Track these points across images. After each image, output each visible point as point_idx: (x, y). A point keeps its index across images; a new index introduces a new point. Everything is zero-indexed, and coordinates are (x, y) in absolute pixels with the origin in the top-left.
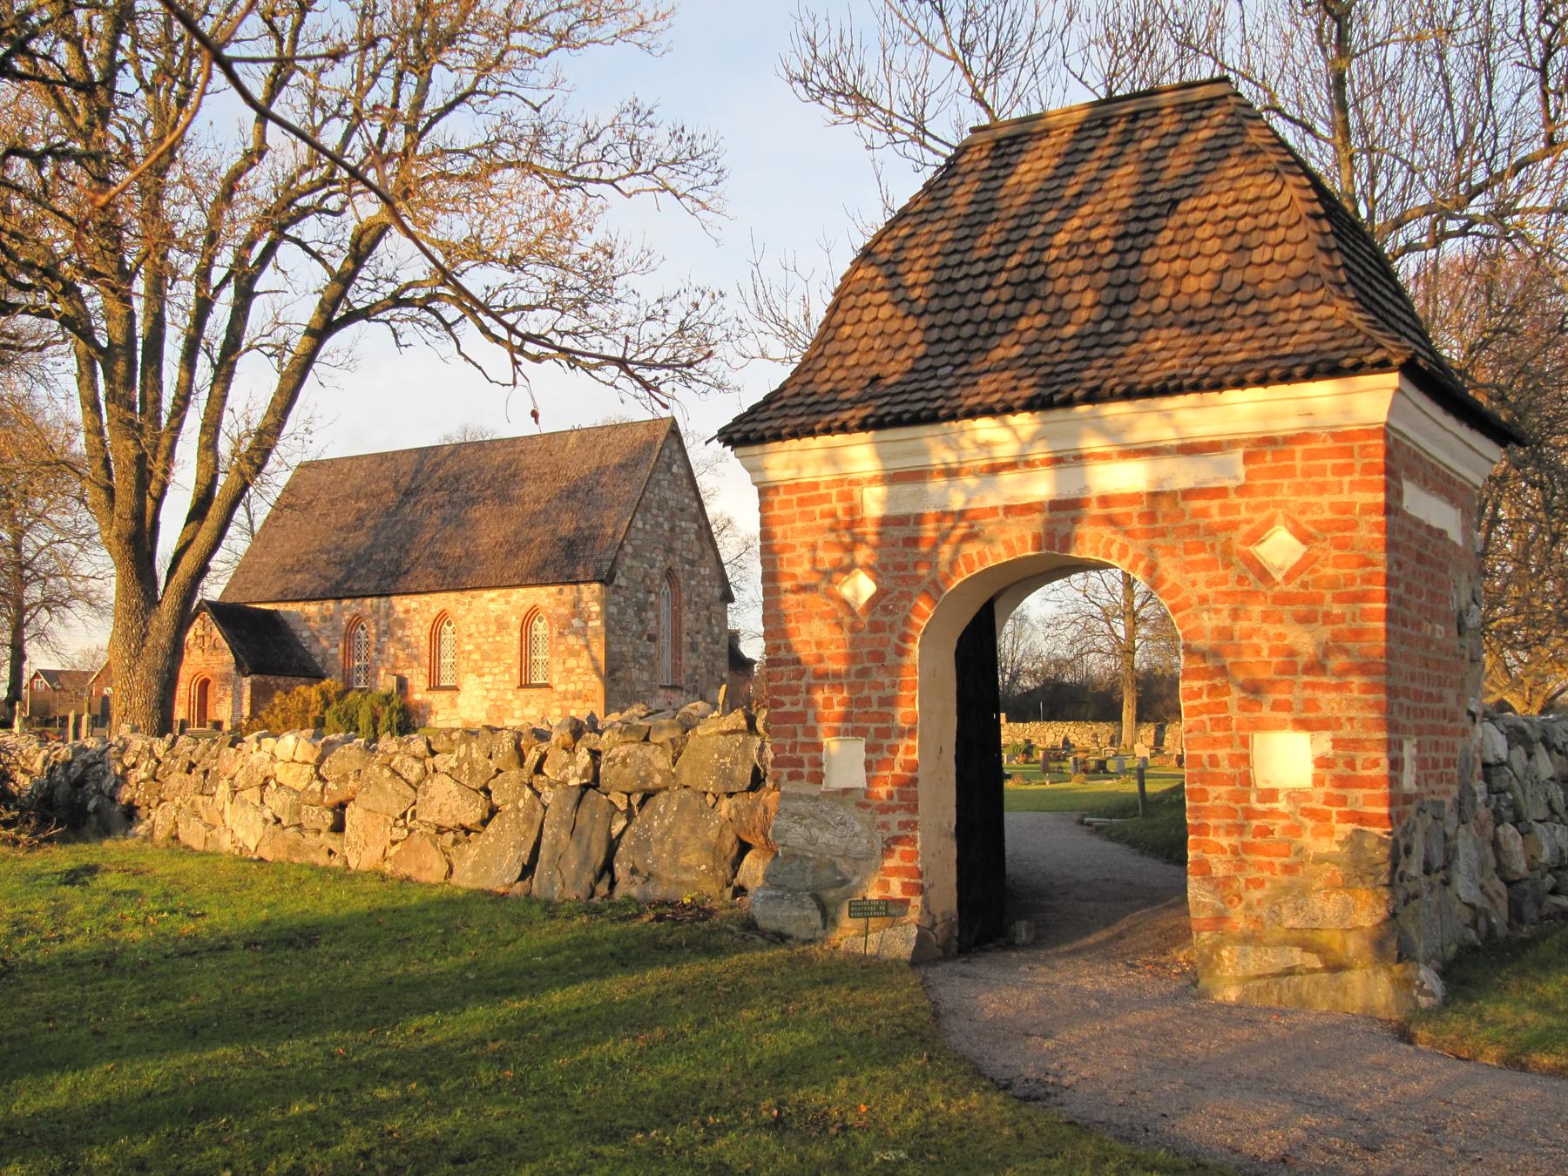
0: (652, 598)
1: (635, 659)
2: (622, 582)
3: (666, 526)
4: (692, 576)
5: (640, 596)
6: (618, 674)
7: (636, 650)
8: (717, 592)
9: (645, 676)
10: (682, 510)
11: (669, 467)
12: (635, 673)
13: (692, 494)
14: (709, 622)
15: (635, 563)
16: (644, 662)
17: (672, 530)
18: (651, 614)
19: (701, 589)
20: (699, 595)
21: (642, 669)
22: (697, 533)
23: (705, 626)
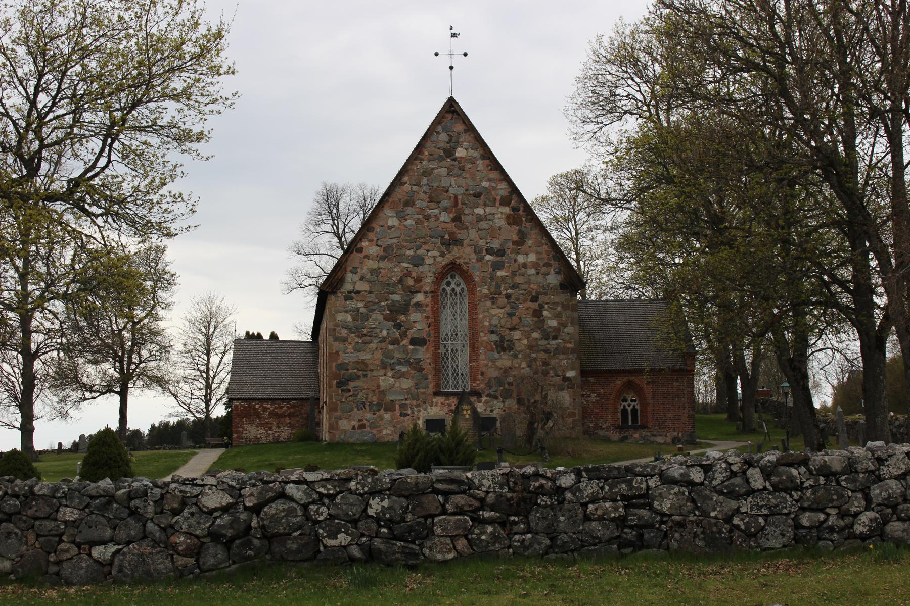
0: (419, 298)
1: (384, 366)
2: (362, 286)
3: (444, 217)
4: (497, 266)
5: (397, 298)
6: (352, 385)
7: (387, 354)
8: (553, 279)
9: (406, 384)
10: (477, 196)
11: (449, 153)
12: (386, 380)
13: (494, 175)
14: (538, 313)
15: (384, 264)
16: (404, 369)
17: (457, 219)
18: (414, 316)
19: (518, 280)
20: (515, 286)
21: (399, 376)
22: (508, 217)
23: (529, 320)
